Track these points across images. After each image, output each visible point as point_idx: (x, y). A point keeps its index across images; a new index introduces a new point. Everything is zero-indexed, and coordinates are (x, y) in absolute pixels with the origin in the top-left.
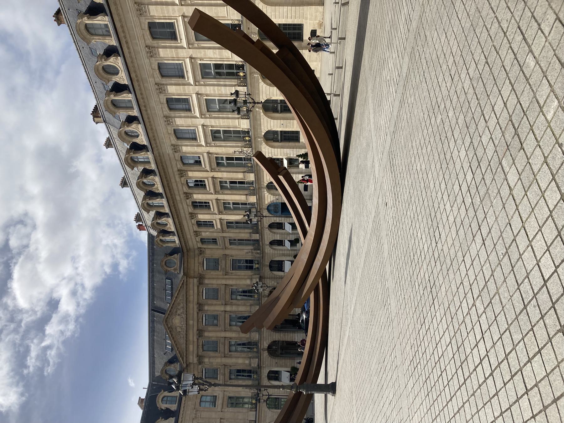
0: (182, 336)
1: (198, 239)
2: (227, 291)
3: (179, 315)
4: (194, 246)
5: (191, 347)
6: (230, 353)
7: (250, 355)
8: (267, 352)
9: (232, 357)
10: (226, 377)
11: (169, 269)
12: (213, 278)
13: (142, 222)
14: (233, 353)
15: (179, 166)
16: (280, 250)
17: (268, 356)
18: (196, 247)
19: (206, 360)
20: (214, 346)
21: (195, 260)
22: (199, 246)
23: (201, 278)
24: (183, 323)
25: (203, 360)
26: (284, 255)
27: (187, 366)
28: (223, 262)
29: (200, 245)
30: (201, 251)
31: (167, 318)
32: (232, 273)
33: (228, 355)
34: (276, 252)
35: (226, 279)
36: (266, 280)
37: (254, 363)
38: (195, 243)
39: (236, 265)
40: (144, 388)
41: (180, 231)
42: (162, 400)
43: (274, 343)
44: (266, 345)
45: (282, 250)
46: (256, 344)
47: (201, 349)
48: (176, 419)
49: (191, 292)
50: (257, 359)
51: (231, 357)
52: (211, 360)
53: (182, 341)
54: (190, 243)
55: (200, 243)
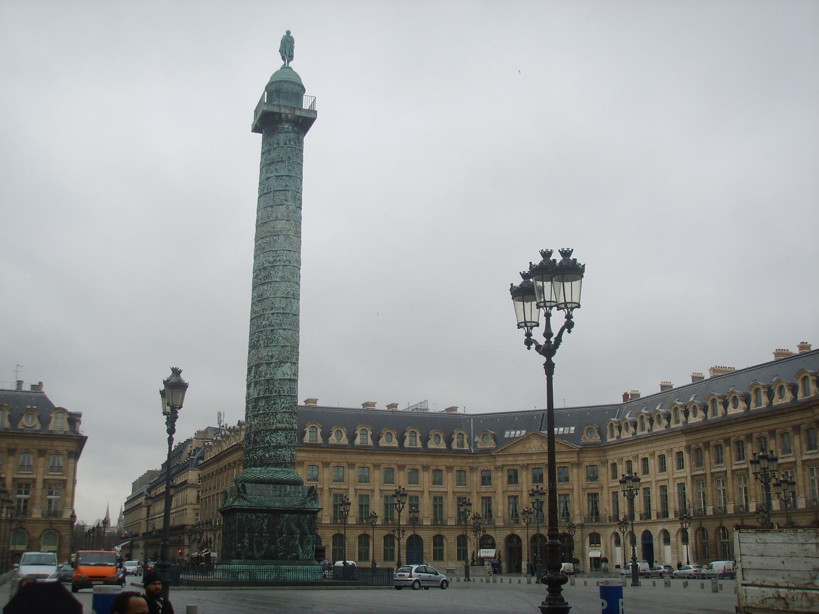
0: (521, 450)
1: (616, 461)
2: (567, 491)
3: (541, 445)
4: (609, 456)
5: (511, 459)
6: (507, 497)
7: (506, 517)
8: (511, 533)
9: (503, 498)
10: (483, 494)
11: (585, 432)
12: (578, 476)
13: (630, 399)
14: (507, 499)
15: (675, 449)
16: (611, 543)
17: (507, 535)
18: (608, 458)
19: (500, 474)
20: (513, 478)
21: (596, 457)
22: (609, 461)
23: (578, 465)
24: (534, 449)
25: (499, 471)
26: (606, 547)
27: (493, 455)
28: (596, 486)
29: (610, 462)
30: (604, 463)
31: (538, 435)
32: (584, 494)
33: (505, 495)
34: (609, 539)
35: (579, 489)
36: (580, 530)
37: (499, 523)
38: (612, 457)
39: (594, 498)
40: (465, 407)
41: (622, 444)
42: (460, 434)
43: (519, 540)
44: (518, 532)
45: (611, 545)
46: (517, 522)
47: (510, 468)
48: (444, 449)
49: (564, 456)
50: (503, 524)
51: (504, 497)
52: (500, 480)
53: (516, 450)
54: (611, 453)
55: (612, 462)
